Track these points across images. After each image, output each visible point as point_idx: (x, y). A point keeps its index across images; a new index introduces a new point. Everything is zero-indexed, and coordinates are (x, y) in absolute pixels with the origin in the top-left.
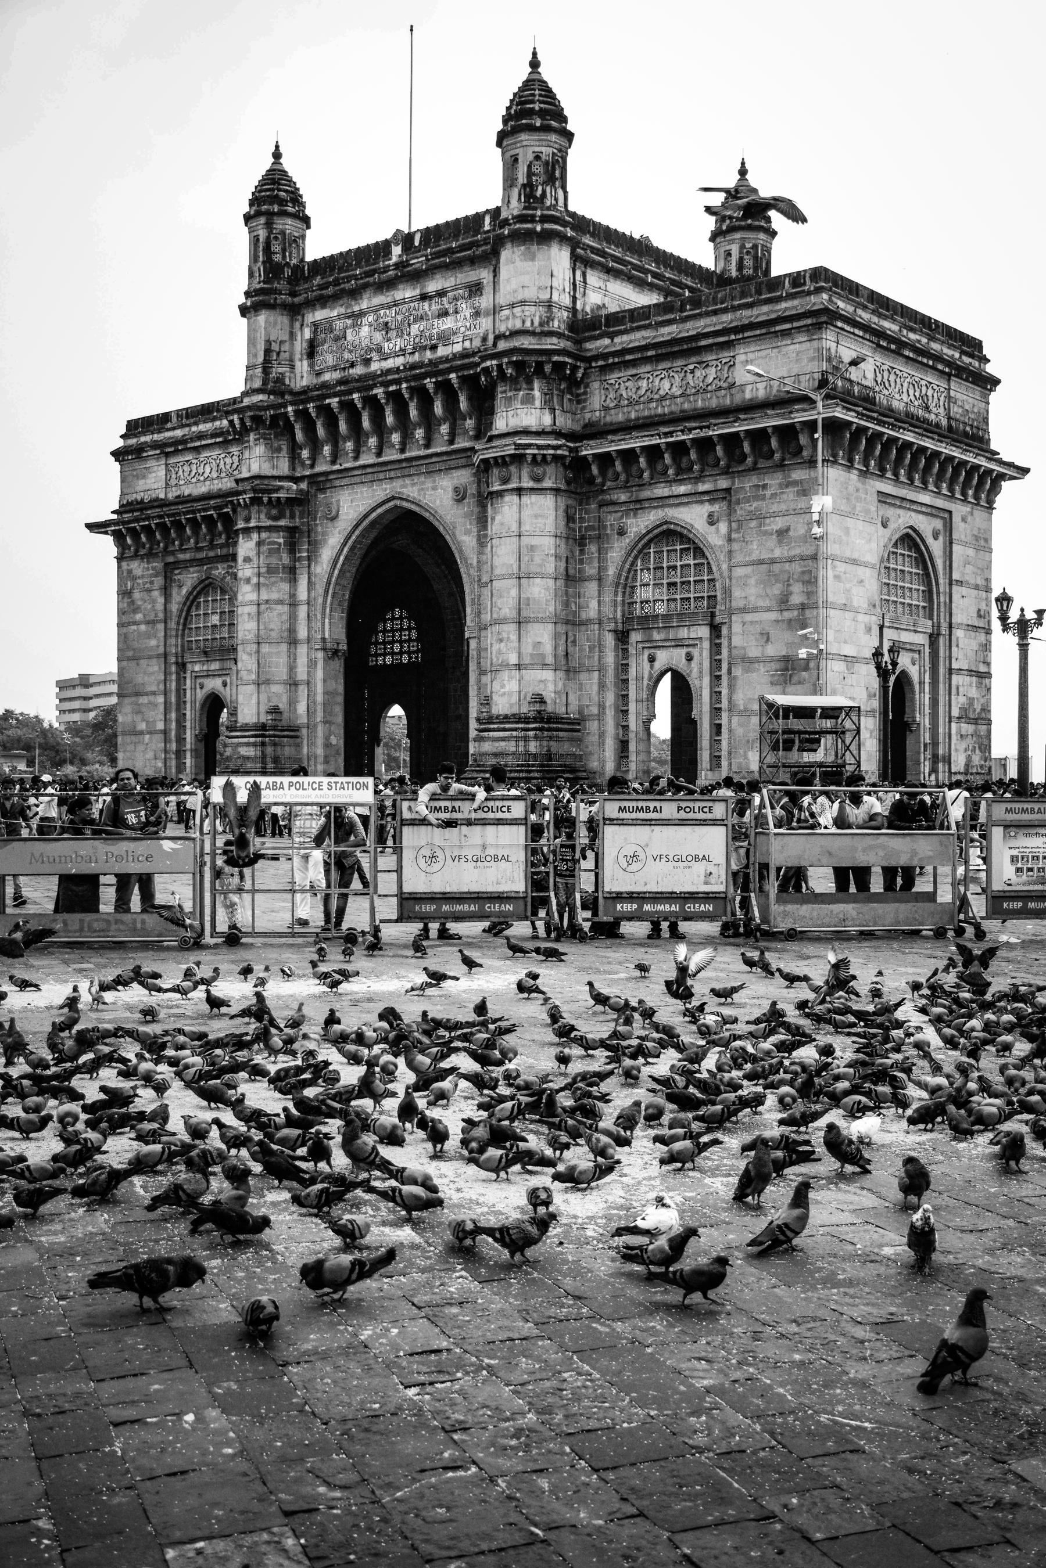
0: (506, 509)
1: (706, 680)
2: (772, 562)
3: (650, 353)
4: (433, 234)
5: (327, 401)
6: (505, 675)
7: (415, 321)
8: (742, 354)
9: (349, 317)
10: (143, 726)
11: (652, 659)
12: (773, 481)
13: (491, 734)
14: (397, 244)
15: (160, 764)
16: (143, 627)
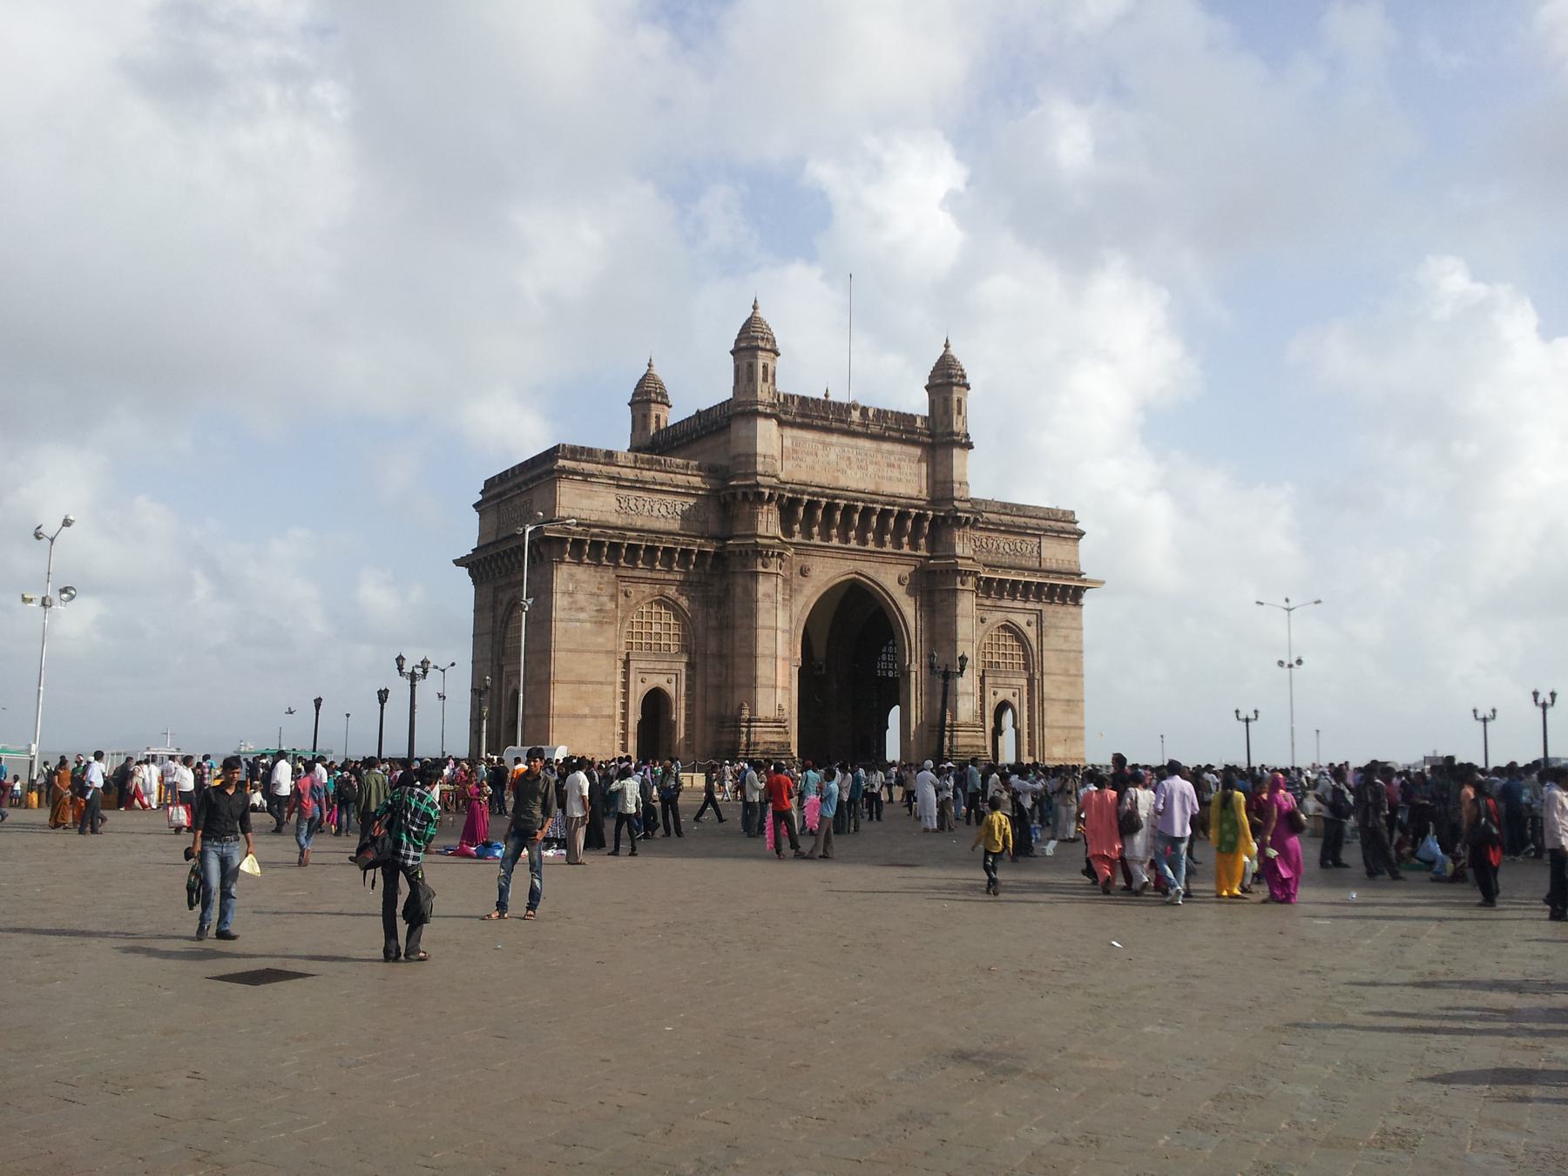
0: (965, 600)
1: (1026, 708)
2: (1062, 651)
3: (1003, 528)
4: (881, 414)
5: (837, 501)
6: (966, 697)
7: (871, 463)
8: (1044, 542)
9: (821, 443)
10: (586, 711)
11: (995, 694)
12: (1061, 610)
13: (959, 733)
14: (855, 409)
15: (606, 744)
16: (588, 625)
